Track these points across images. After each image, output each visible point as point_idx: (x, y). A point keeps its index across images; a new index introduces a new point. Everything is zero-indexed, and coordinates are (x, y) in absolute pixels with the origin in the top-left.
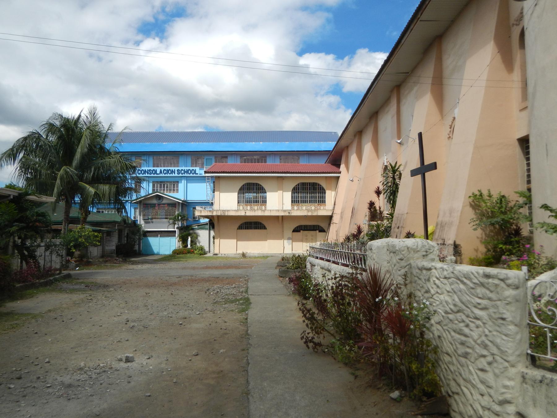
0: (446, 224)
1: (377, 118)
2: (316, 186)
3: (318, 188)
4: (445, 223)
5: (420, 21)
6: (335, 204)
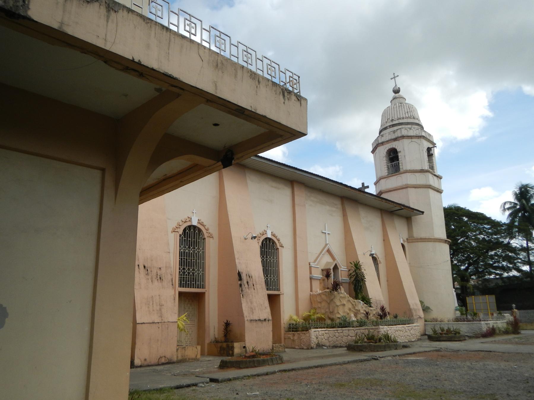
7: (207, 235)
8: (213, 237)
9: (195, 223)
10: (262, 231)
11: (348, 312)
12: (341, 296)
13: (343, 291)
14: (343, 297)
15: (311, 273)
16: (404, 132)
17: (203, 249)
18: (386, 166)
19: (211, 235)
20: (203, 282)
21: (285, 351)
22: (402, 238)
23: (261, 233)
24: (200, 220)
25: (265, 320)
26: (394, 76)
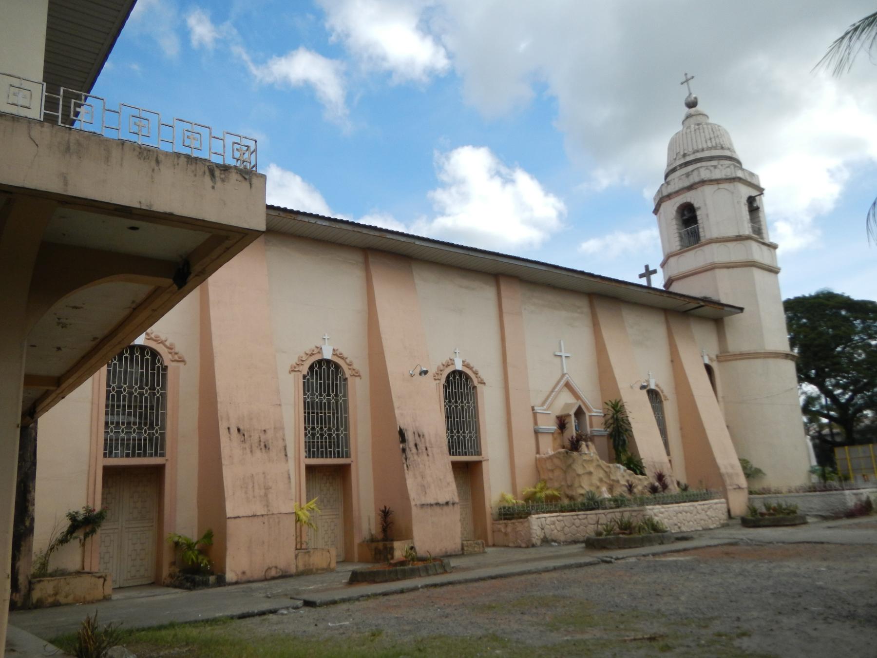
7: (351, 372)
8: (359, 376)
9: (327, 355)
10: (447, 361)
11: (599, 484)
12: (584, 458)
13: (589, 451)
14: (589, 461)
15: (536, 423)
16: (705, 174)
17: (345, 396)
18: (677, 235)
19: (357, 373)
20: (346, 447)
21: (484, 552)
22: (708, 355)
23: (444, 363)
24: (337, 350)
25: (447, 503)
26: (686, 77)
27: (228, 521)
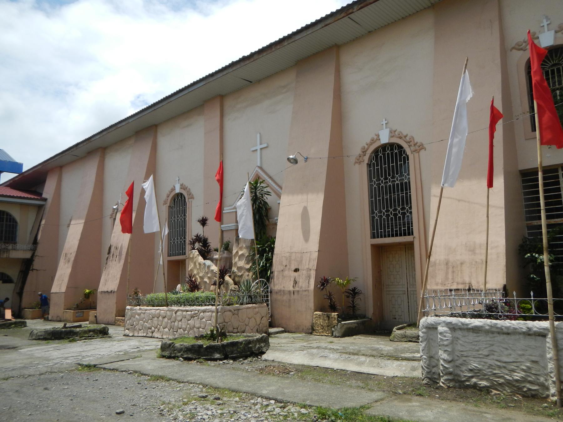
0: (462, 264)
1: (156, 132)
2: (3, 215)
3: (7, 219)
4: (458, 263)
5: (349, 17)
6: (35, 242)
25: (111, 291)
27: (51, 294)
